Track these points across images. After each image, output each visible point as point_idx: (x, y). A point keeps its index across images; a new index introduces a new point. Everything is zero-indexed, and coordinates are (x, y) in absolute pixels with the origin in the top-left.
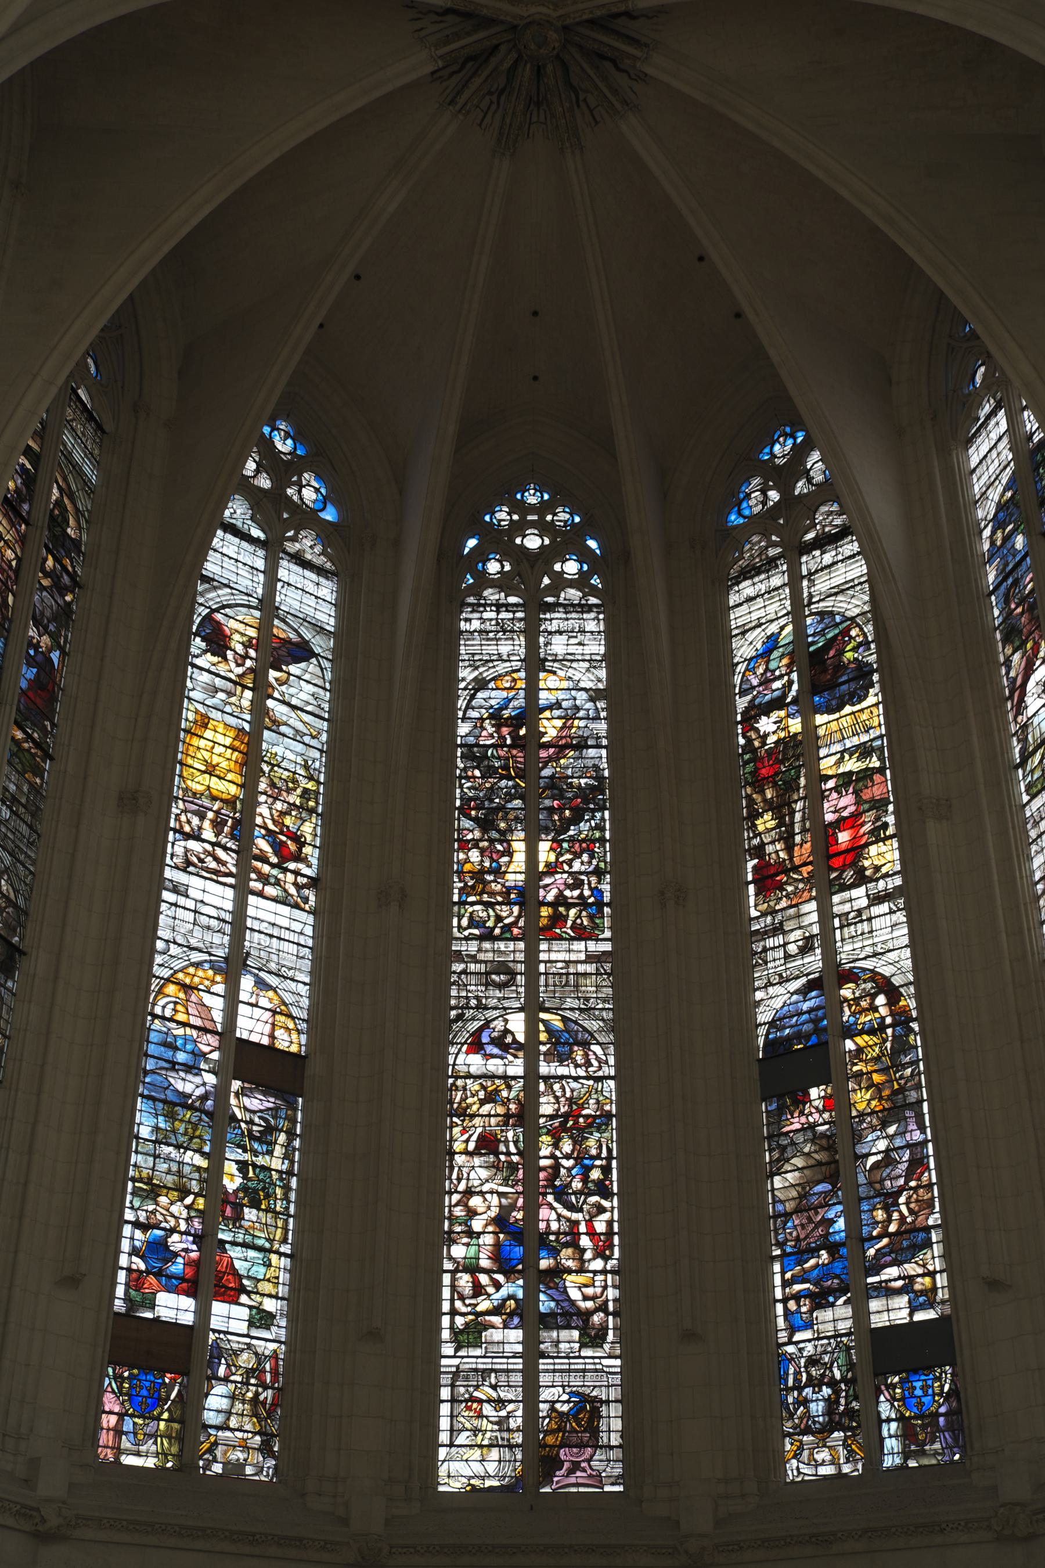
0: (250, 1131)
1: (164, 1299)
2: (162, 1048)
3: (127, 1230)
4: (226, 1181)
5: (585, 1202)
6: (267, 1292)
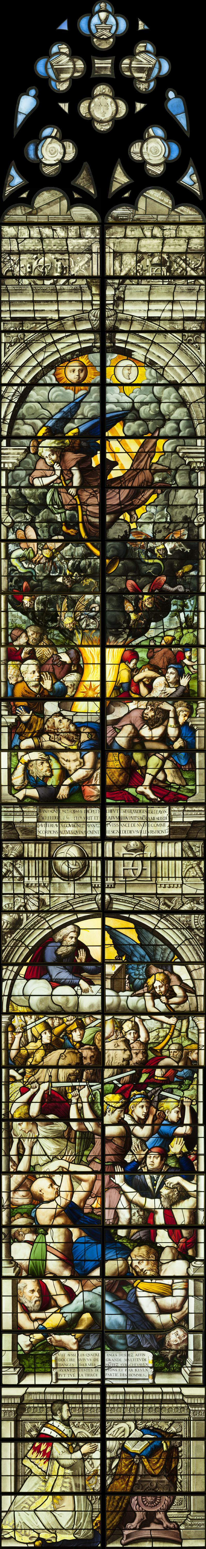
5: (163, 1183)
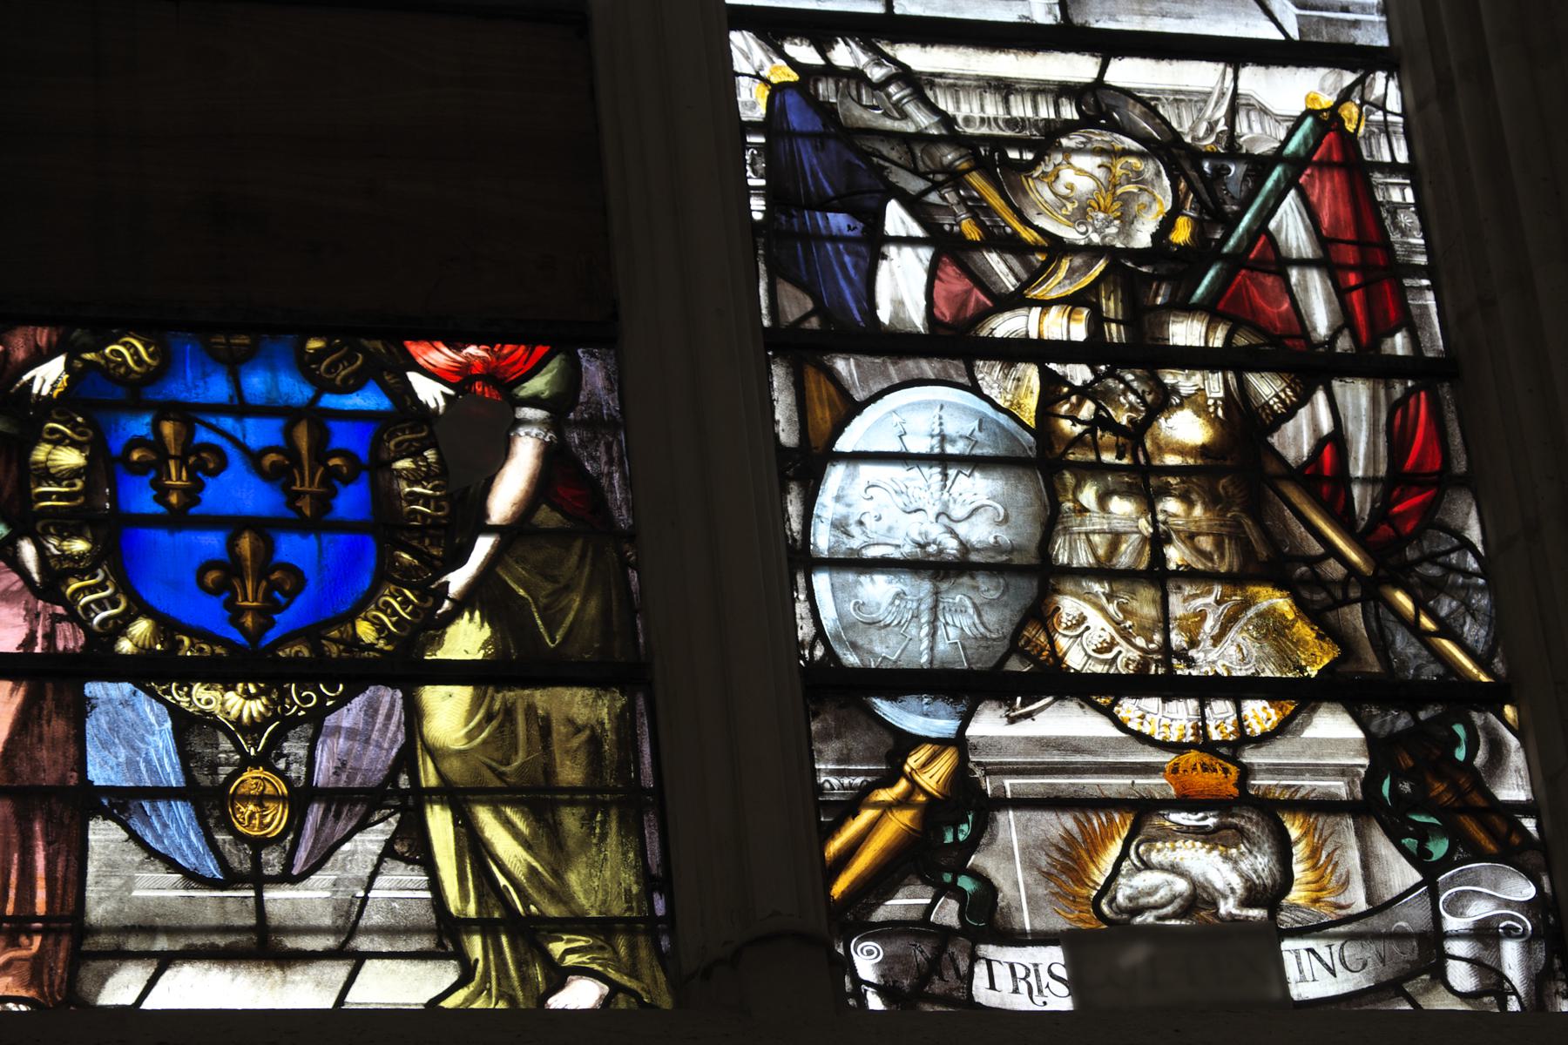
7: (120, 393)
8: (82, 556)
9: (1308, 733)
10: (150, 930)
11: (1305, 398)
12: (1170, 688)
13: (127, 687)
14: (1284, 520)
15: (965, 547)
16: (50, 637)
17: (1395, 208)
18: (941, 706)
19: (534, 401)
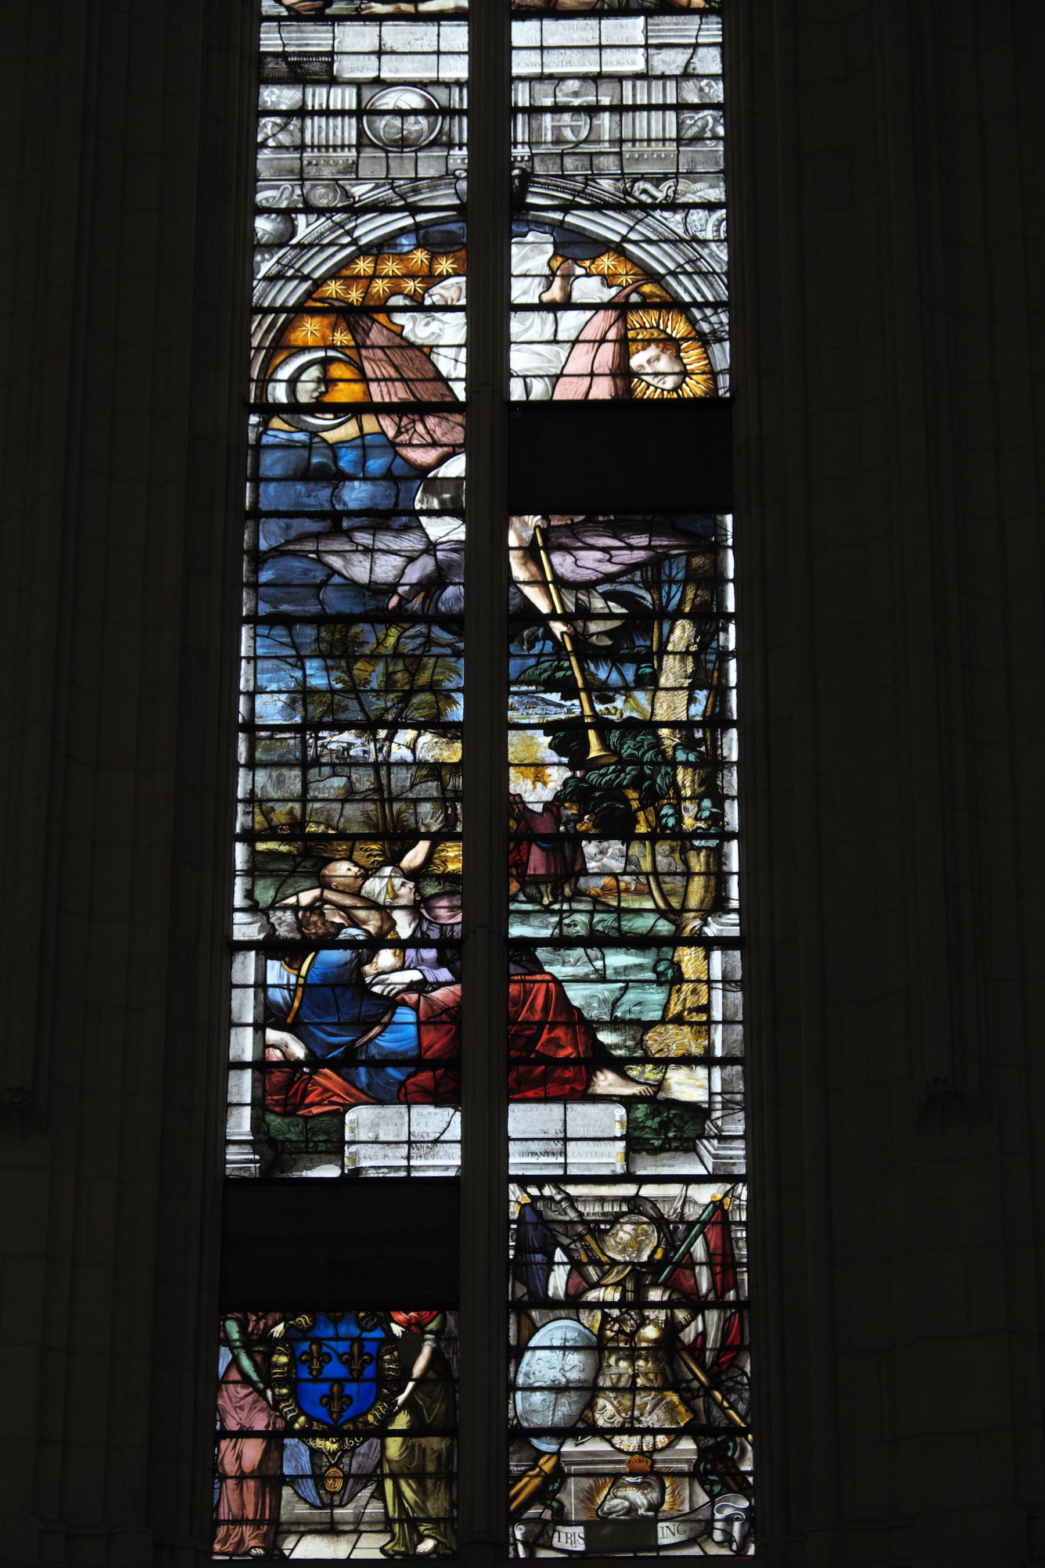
0: (580, 640)
1: (362, 1120)
2: (300, 487)
3: (244, 969)
4: (519, 784)
6: (675, 1052)
7: (300, 1335)
8: (285, 1395)
9: (678, 1447)
10: (298, 1523)
11: (694, 1318)
12: (632, 1431)
13: (296, 1440)
14: (680, 1366)
15: (568, 1381)
16: (274, 1423)
17: (738, 1239)
18: (553, 1441)
19: (431, 1332)
